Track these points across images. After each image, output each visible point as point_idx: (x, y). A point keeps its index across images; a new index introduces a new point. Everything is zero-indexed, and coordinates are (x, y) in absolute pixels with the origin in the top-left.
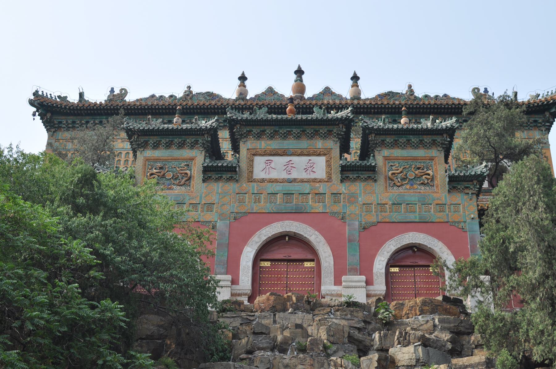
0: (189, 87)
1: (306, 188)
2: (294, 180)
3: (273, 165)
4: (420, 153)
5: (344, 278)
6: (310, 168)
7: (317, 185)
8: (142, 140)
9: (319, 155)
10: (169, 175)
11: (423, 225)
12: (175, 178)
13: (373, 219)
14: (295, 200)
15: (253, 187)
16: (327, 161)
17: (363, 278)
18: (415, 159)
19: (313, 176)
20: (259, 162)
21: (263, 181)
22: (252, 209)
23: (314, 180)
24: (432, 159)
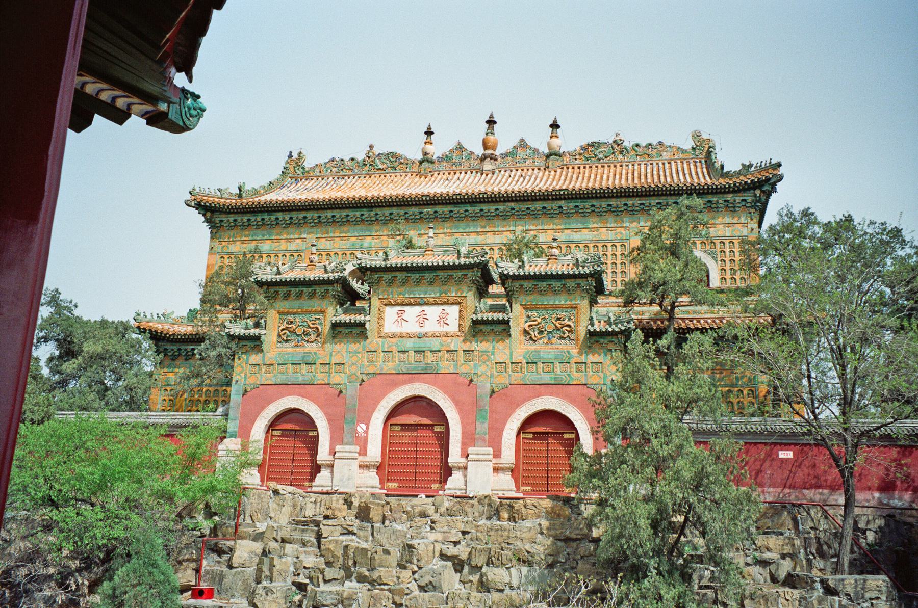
0: (371, 147)
1: (435, 344)
2: (426, 335)
3: (405, 316)
4: (562, 300)
5: (471, 450)
6: (443, 320)
7: (449, 340)
8: (273, 290)
9: (453, 304)
10: (299, 331)
11: (558, 387)
12: (306, 334)
13: (504, 380)
14: (429, 358)
15: (383, 344)
16: (460, 311)
17: (491, 450)
18: (556, 308)
19: (446, 329)
20: (391, 313)
21: (394, 336)
22: (382, 370)
23: (446, 335)
24: (574, 307)
